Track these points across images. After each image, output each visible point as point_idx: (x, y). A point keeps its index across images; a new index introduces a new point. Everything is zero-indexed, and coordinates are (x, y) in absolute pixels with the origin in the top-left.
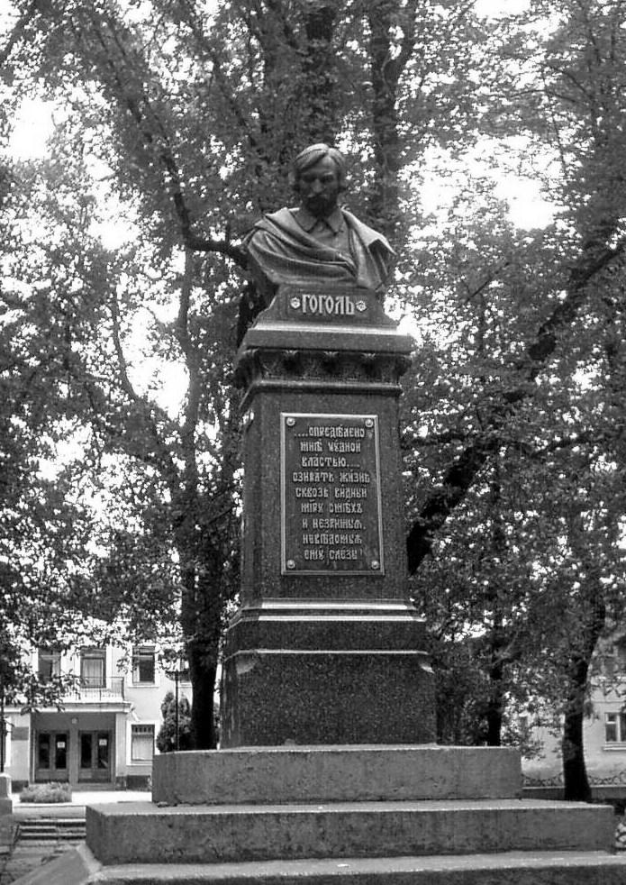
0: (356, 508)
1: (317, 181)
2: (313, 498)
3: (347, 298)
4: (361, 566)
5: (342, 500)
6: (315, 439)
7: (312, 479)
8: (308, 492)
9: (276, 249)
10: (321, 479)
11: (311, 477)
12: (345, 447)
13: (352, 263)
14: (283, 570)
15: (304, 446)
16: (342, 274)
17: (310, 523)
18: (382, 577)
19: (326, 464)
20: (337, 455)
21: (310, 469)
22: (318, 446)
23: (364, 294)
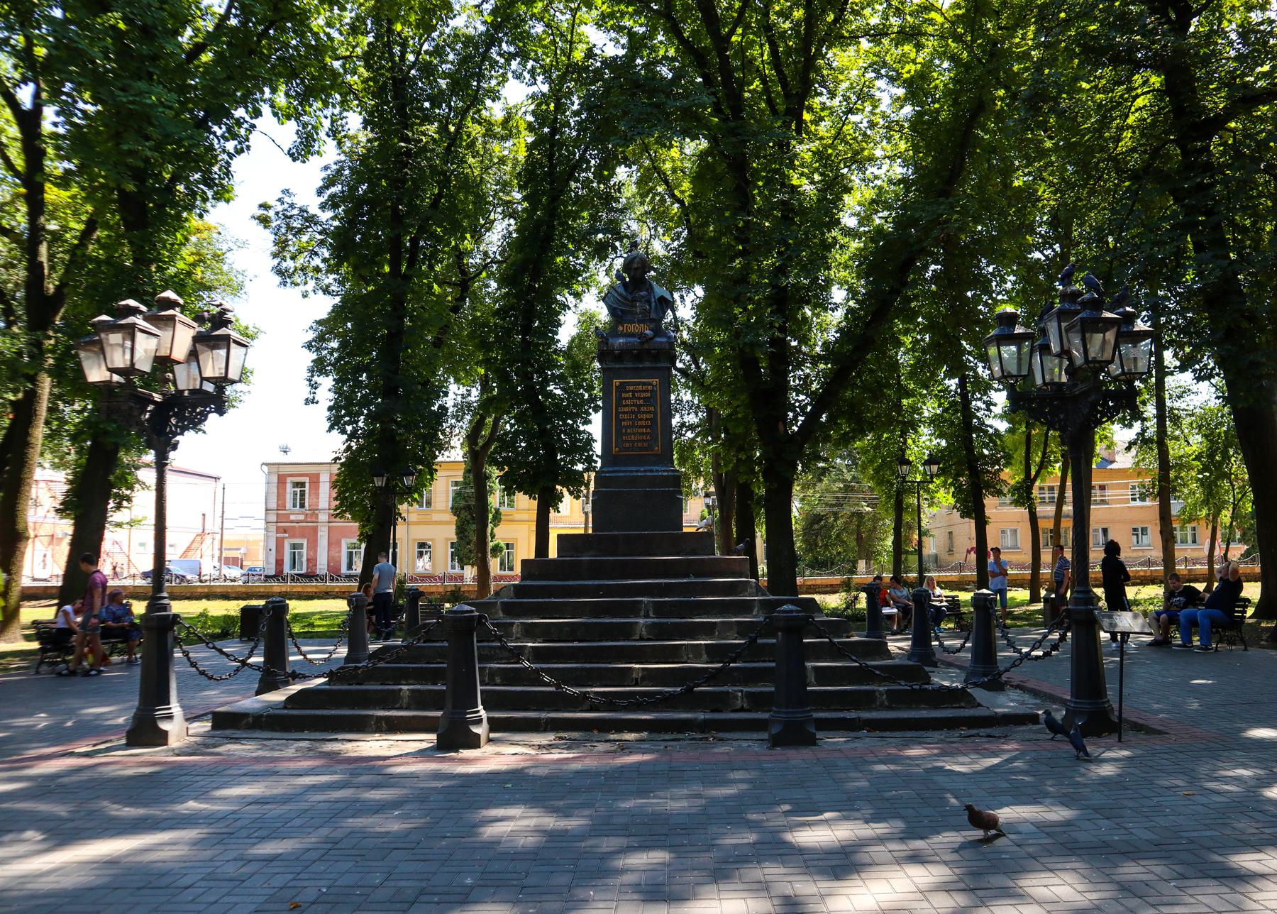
8: (626, 416)
11: (625, 409)
12: (643, 395)
20: (639, 398)
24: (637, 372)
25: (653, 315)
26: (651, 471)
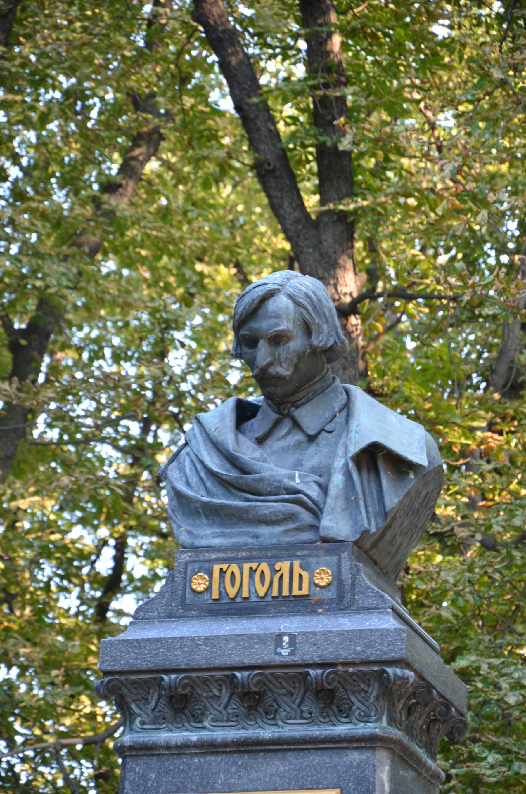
1: (262, 343)
3: (297, 563)
9: (194, 480)
13: (314, 492)
16: (291, 517)
23: (329, 552)
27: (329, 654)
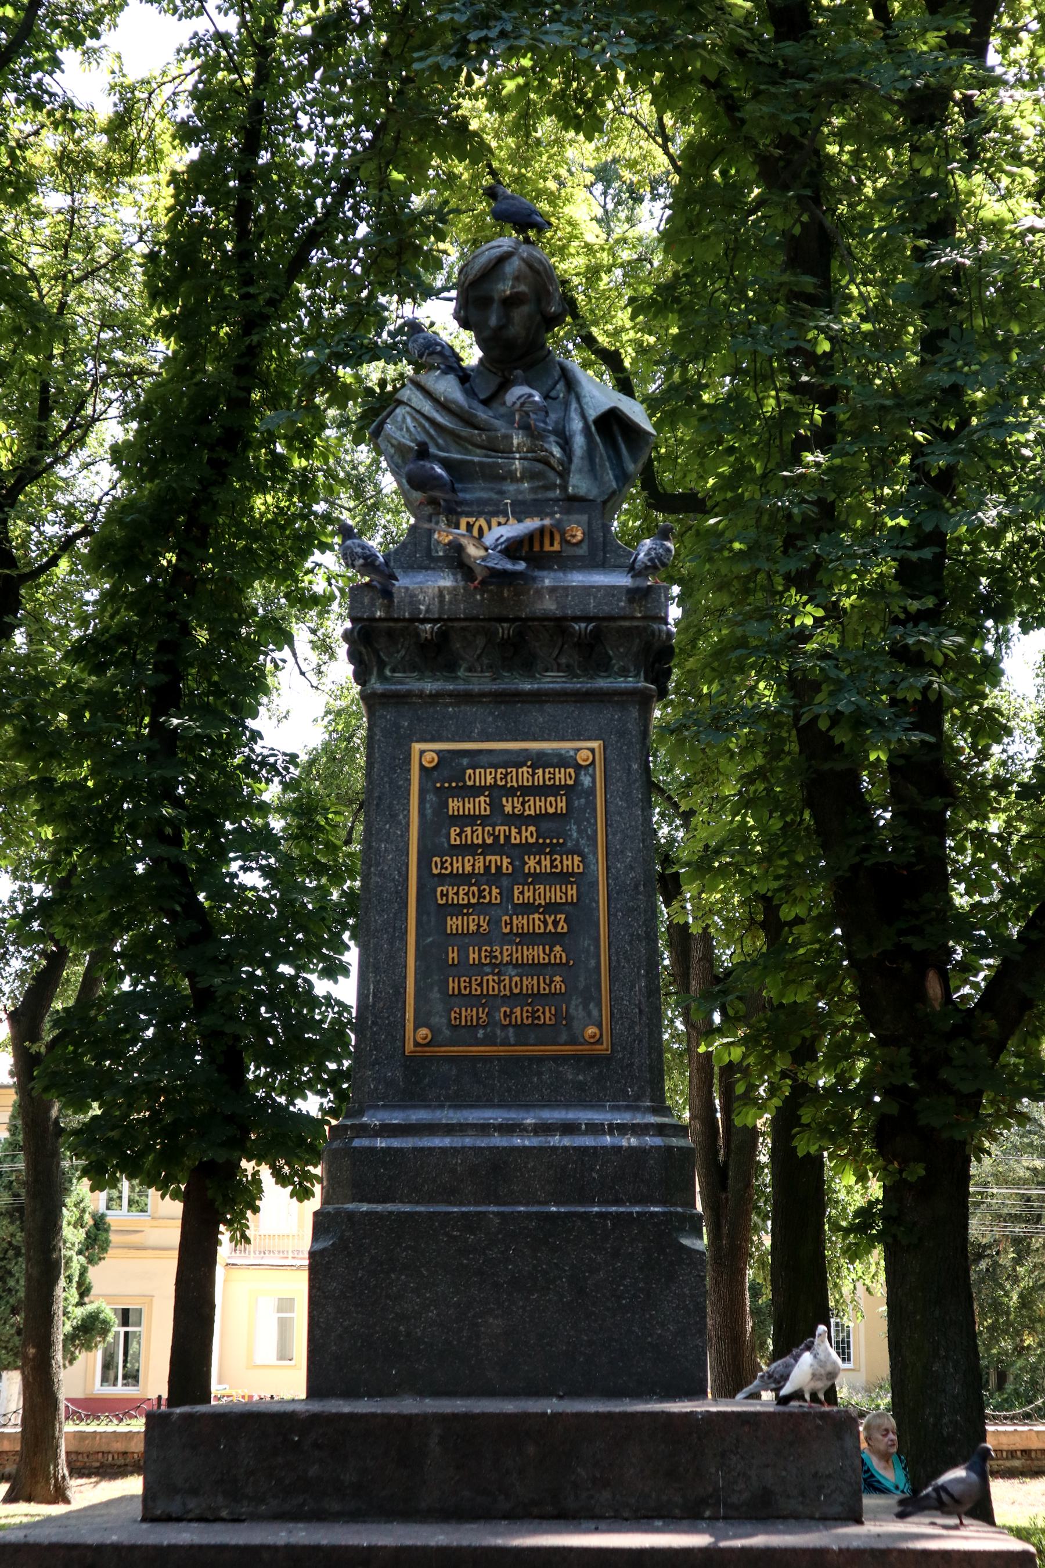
0: (555, 923)
2: (469, 905)
4: (564, 1037)
5: (528, 908)
6: (476, 791)
7: (468, 869)
8: (461, 895)
10: (487, 868)
11: (465, 865)
12: (535, 805)
14: (410, 1046)
15: (454, 805)
17: (463, 952)
18: (608, 1059)
19: (497, 838)
20: (519, 820)
21: (469, 849)
22: (481, 805)
23: (581, 512)
24: (511, 709)
25: (579, 483)
26: (569, 1128)
27: (592, 607)
